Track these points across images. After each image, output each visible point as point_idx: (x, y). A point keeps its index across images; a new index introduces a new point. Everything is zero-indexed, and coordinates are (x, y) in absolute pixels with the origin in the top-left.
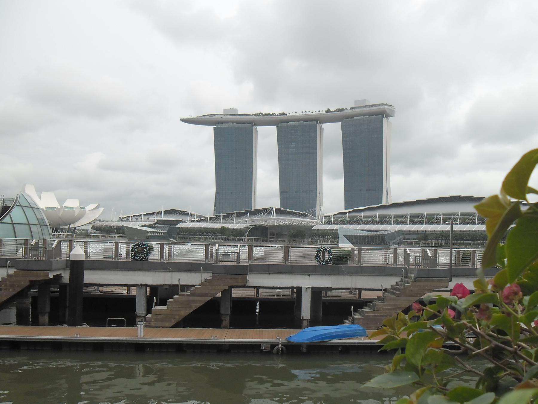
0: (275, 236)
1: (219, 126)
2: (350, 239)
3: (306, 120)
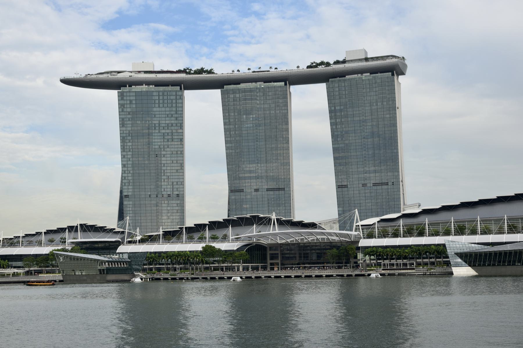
0: (279, 261)
1: (127, 89)
2: (470, 258)
3: (267, 80)
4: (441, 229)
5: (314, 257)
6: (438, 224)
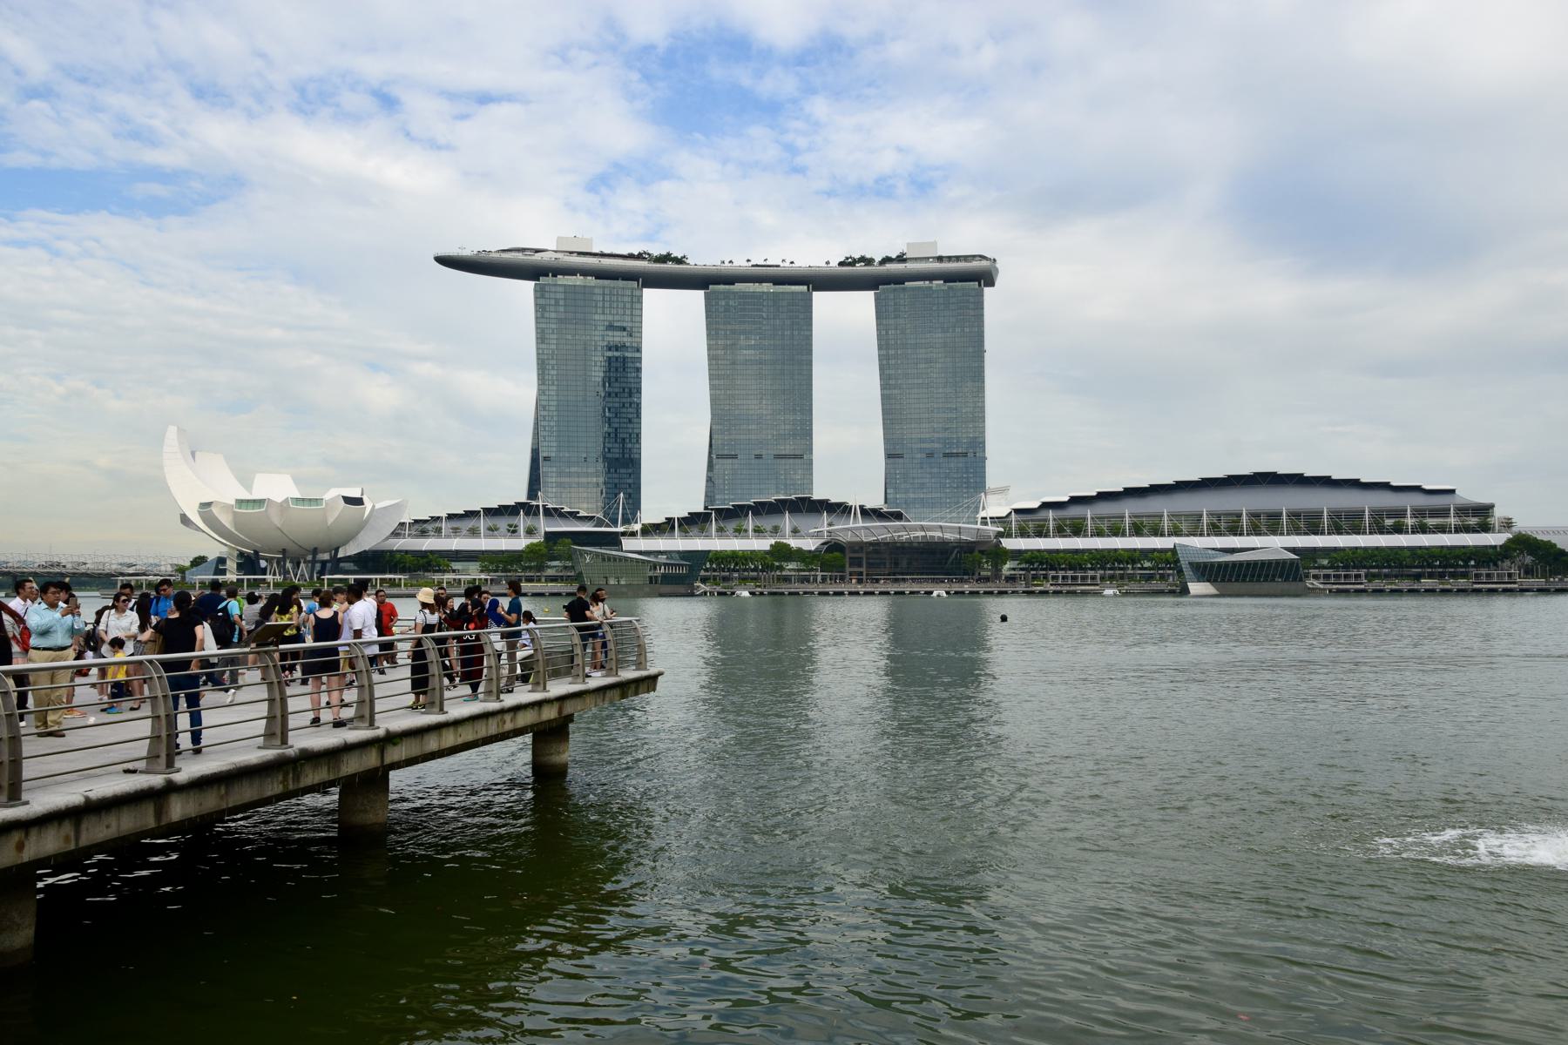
0: (863, 569)
1: (549, 280)
4: (1105, 526)
5: (904, 564)
6: (1101, 518)
